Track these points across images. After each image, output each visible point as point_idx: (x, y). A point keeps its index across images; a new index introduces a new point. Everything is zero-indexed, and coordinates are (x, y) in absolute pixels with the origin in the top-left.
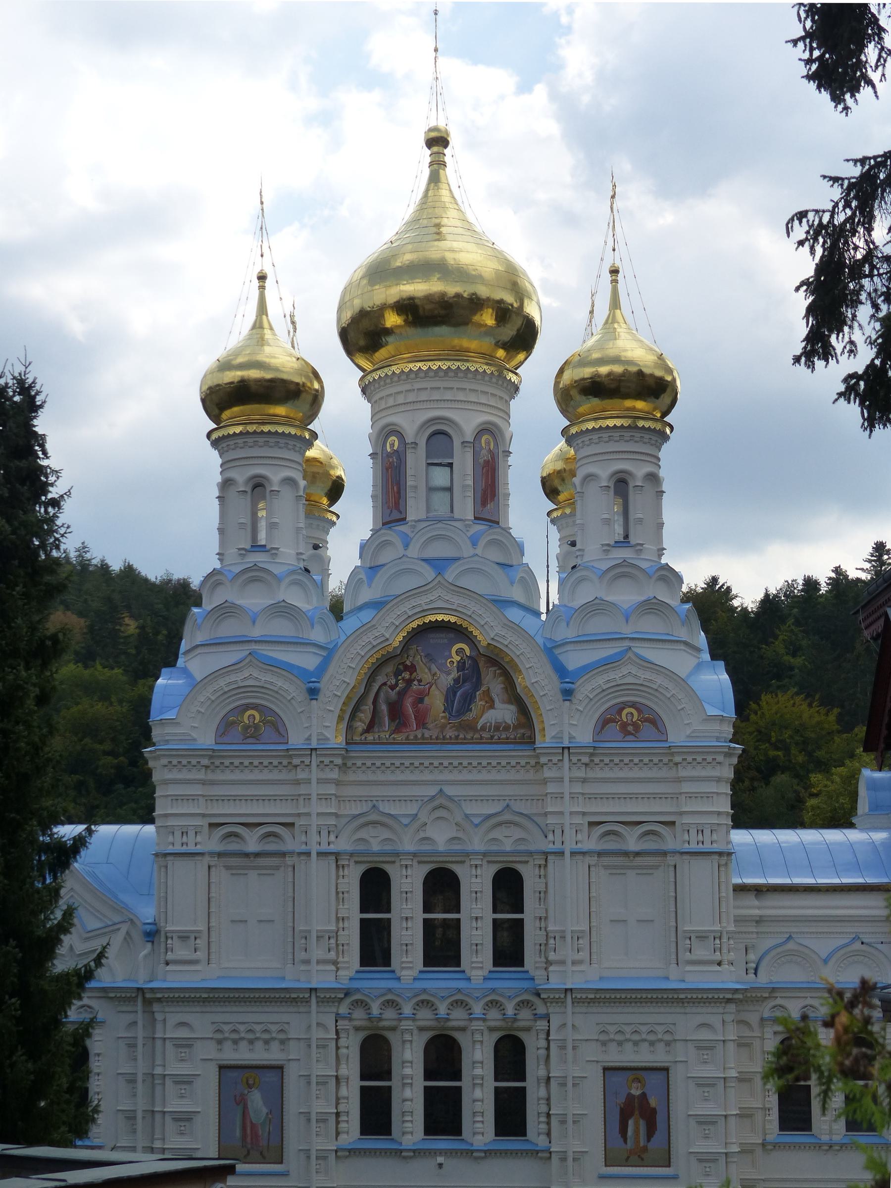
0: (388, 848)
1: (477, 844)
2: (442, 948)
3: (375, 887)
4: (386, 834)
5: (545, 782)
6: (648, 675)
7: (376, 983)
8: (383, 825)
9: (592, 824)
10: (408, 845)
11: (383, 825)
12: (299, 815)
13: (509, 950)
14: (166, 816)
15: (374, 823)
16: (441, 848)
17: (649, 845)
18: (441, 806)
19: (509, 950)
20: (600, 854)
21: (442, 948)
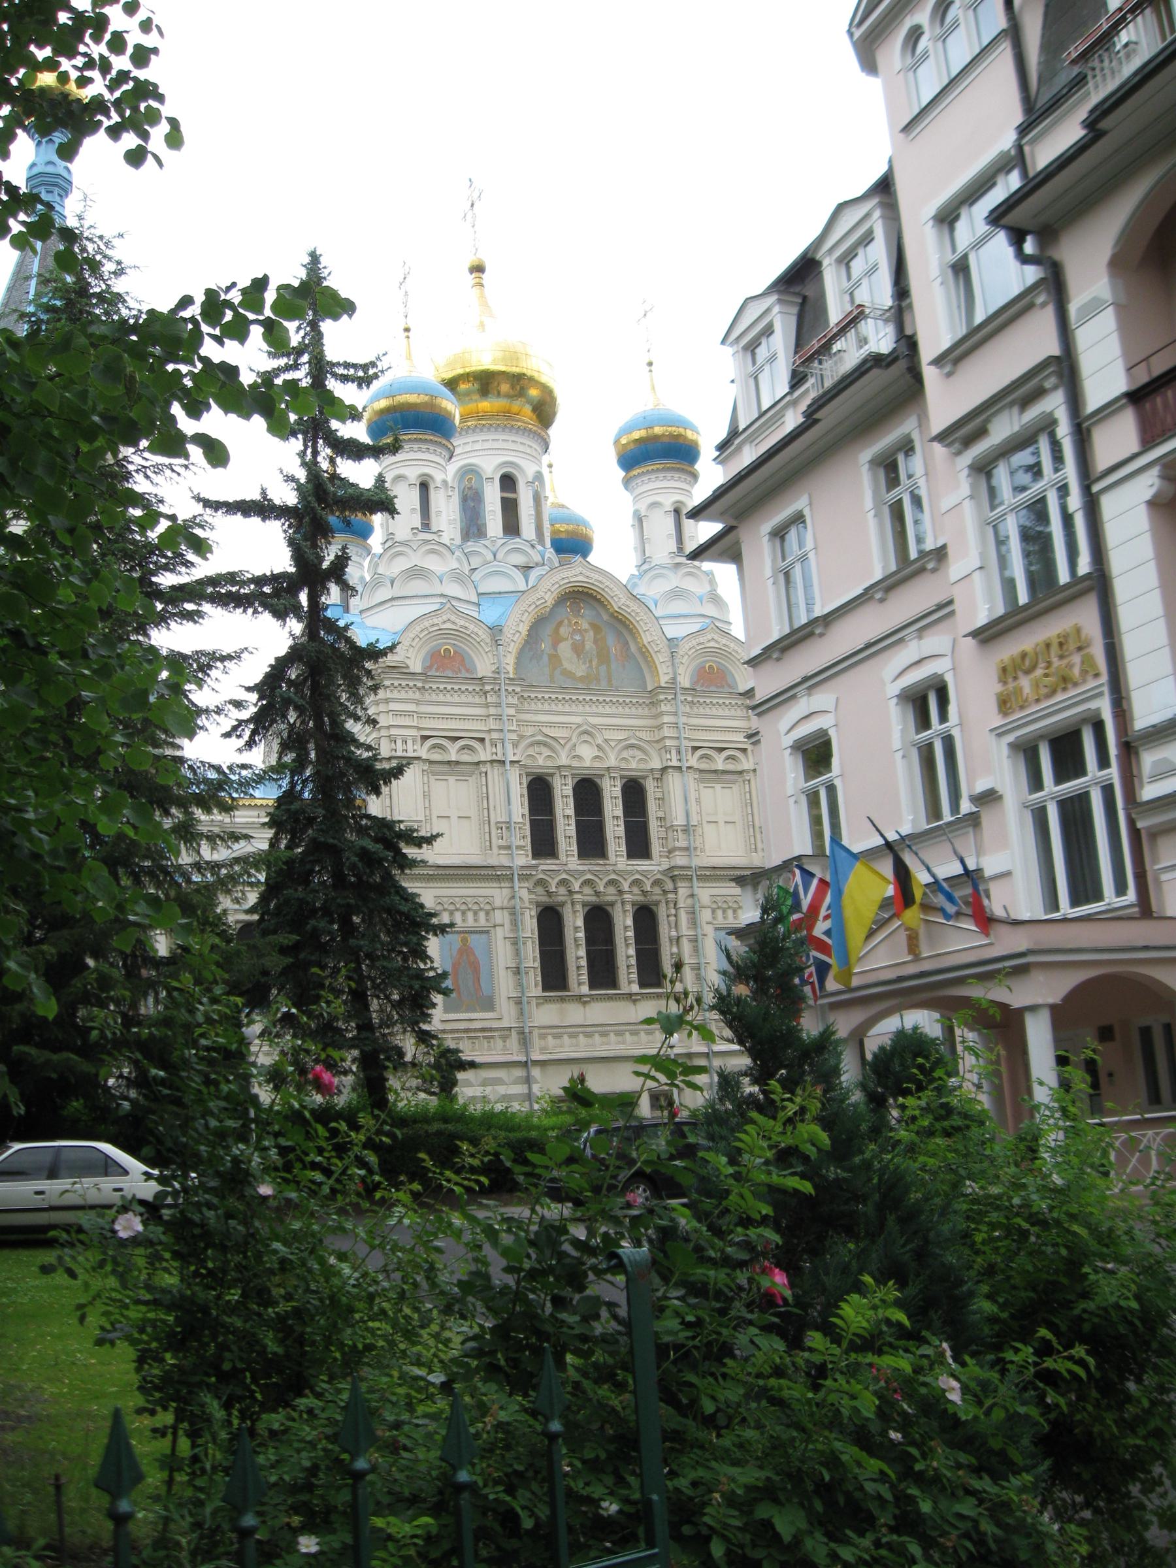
0: (549, 763)
1: (612, 761)
2: (592, 842)
3: (539, 791)
4: (546, 752)
5: (661, 714)
6: (724, 641)
7: (547, 865)
8: (545, 744)
9: (695, 749)
10: (564, 760)
11: (545, 744)
12: (489, 731)
13: (639, 845)
14: (388, 727)
15: (539, 743)
16: (588, 764)
17: (730, 766)
18: (586, 732)
19: (639, 845)
20: (701, 771)
21: (592, 842)
